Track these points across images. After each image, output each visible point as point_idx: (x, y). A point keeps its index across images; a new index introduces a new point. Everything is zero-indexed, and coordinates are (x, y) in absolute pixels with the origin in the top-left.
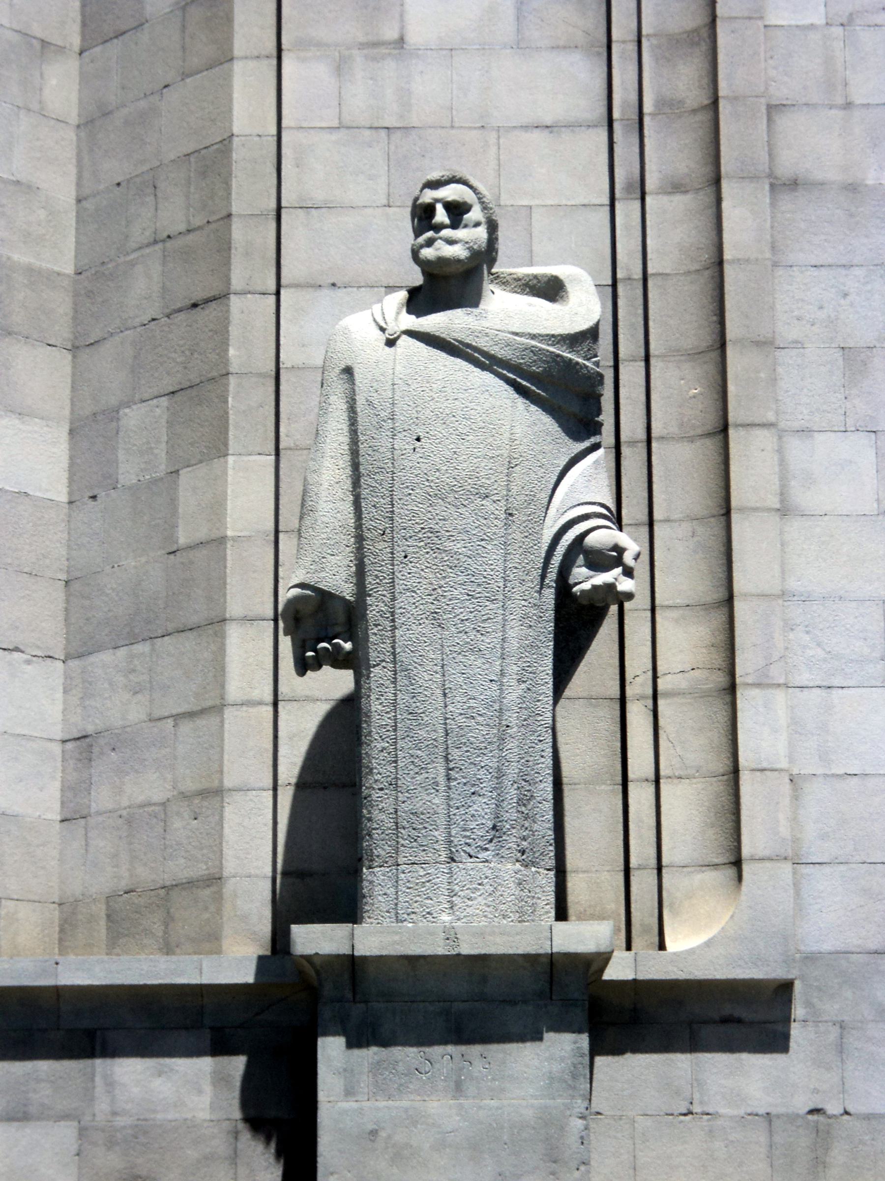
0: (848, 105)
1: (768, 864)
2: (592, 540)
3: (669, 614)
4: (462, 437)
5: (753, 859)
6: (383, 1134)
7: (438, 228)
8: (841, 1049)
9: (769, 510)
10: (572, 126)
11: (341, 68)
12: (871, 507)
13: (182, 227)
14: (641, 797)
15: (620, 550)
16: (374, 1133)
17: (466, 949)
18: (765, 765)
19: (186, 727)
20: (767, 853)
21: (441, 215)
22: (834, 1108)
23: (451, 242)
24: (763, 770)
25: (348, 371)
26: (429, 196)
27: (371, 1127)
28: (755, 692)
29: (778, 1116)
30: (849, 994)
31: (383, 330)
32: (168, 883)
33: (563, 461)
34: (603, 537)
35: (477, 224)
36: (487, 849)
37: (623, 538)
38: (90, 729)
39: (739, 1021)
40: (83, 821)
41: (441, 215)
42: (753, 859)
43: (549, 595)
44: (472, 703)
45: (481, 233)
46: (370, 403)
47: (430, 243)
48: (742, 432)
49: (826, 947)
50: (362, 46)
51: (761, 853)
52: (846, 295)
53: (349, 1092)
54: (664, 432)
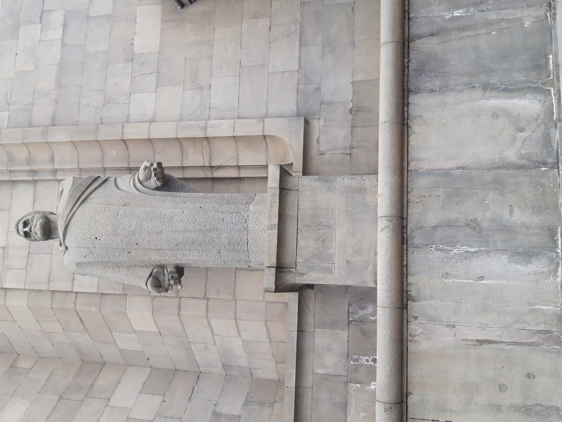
0: (32, 104)
1: (265, 126)
2: (141, 177)
3: (184, 162)
4: (96, 222)
5: (263, 132)
6: (348, 258)
7: (30, 230)
8: (329, 103)
9: (150, 126)
10: (35, 193)
11: (9, 268)
12: (154, 95)
13: (59, 324)
14: (244, 174)
15: (146, 168)
16: (348, 262)
17: (276, 222)
18: (232, 128)
19: (216, 332)
20: (262, 127)
21: (27, 229)
22: (351, 105)
23: (35, 226)
24: (234, 128)
25: (78, 265)
26: (22, 234)
27: (345, 264)
28: (209, 131)
29: (352, 124)
30: (311, 101)
31: (64, 252)
32: (269, 341)
33: (115, 188)
34: (141, 174)
35: (33, 217)
36: (244, 216)
37: (142, 167)
38: (221, 365)
39: (319, 138)
40: (252, 370)
41: (27, 229)
42: (263, 132)
43: (158, 193)
44: (190, 220)
45: (36, 216)
46: (85, 256)
47: (36, 233)
48: (124, 135)
49: (295, 108)
50: (3, 261)
51: (261, 129)
52: (88, 104)
53: (330, 271)
54: (127, 163)
